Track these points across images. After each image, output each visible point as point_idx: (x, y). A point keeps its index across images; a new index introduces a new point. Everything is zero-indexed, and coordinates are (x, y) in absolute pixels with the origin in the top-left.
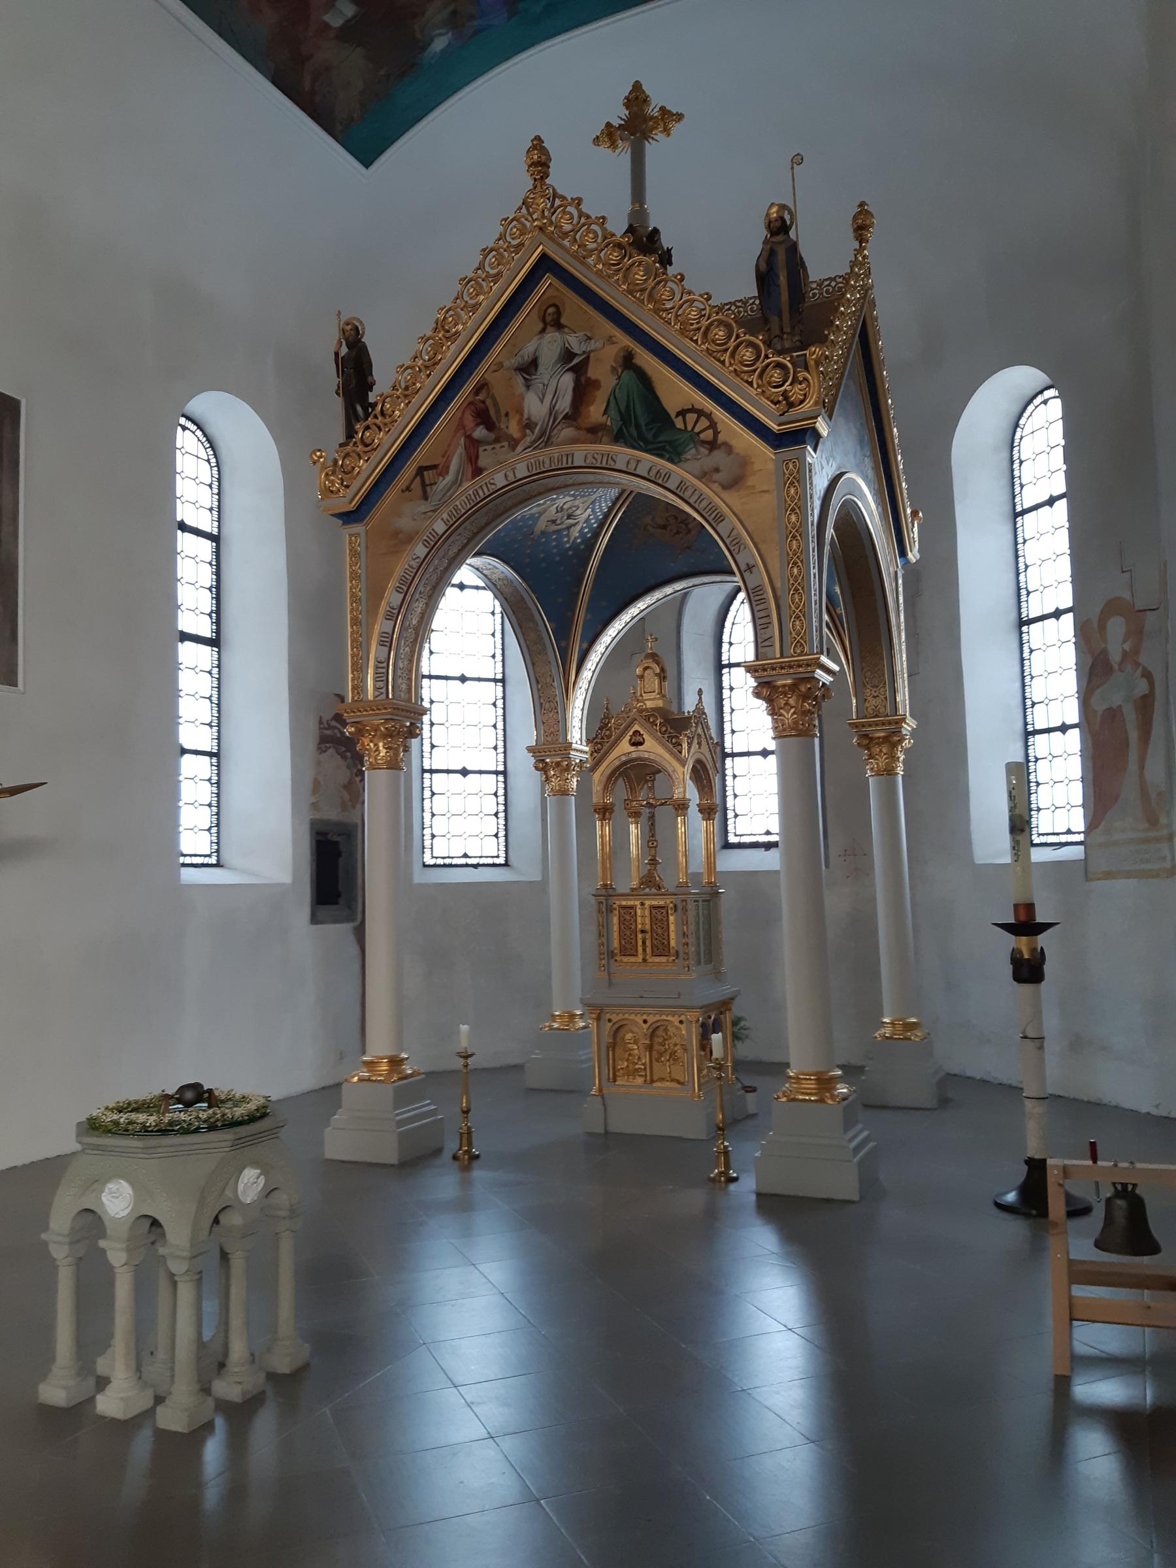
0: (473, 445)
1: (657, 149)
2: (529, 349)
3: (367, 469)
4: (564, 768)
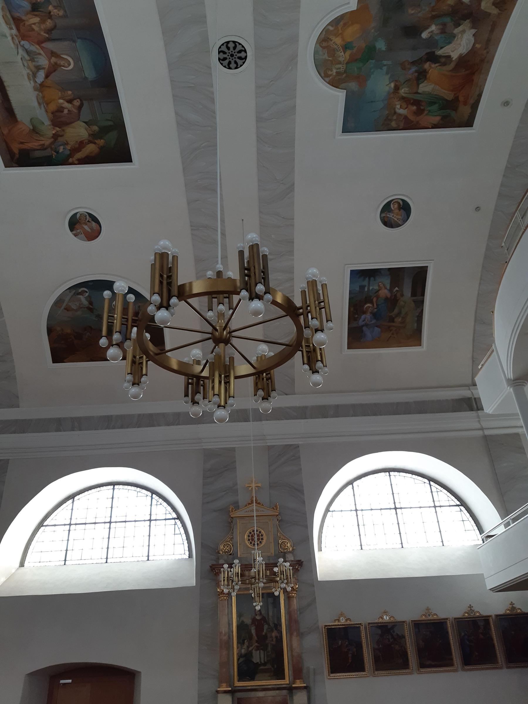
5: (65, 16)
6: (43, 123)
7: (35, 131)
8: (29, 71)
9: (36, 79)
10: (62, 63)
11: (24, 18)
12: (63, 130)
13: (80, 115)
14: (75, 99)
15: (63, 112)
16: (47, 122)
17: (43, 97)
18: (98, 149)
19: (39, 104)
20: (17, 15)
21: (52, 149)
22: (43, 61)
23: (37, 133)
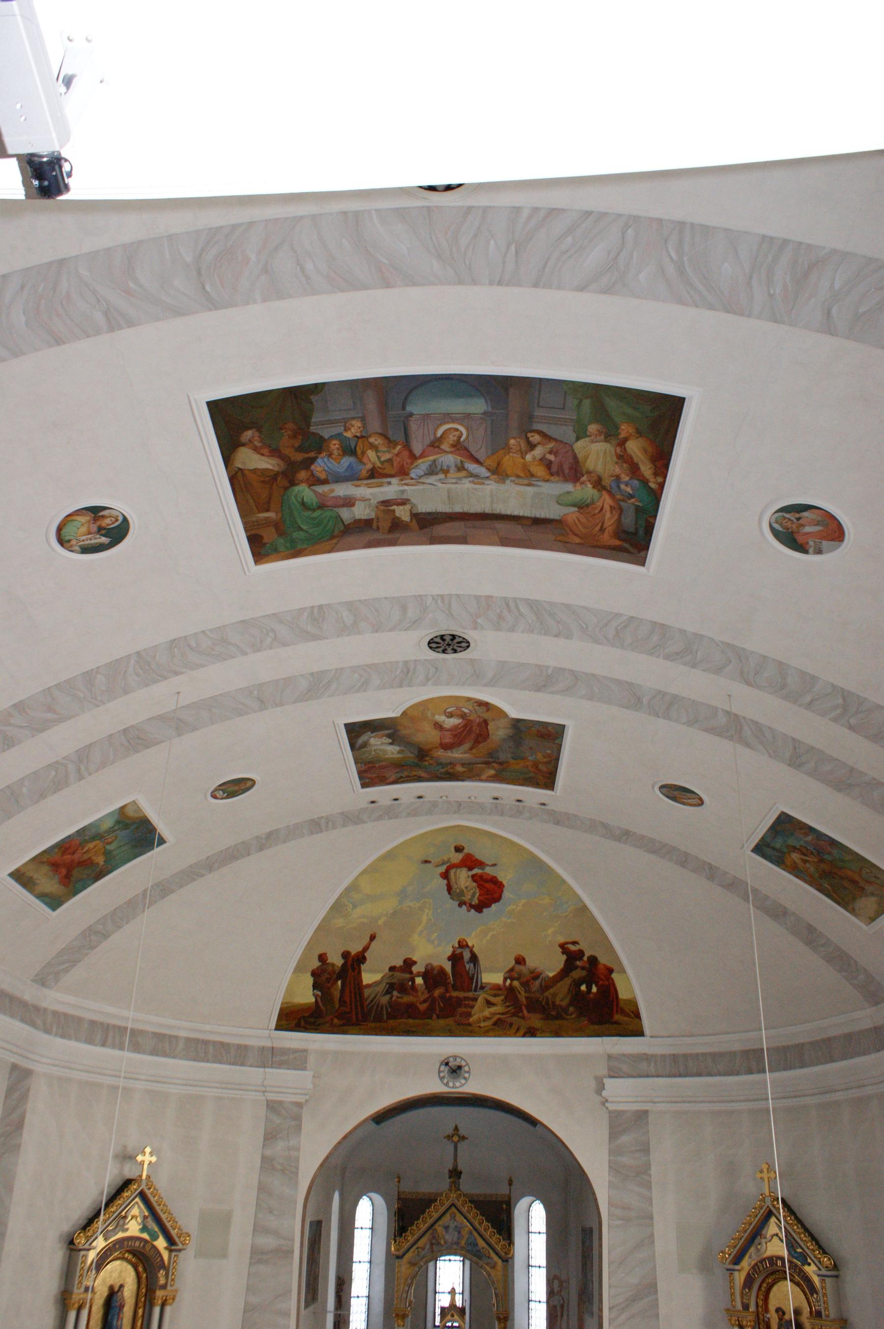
0: (432, 1244)
1: (462, 1146)
2: (447, 1224)
5: (363, 419)
6: (568, 493)
7: (582, 506)
8: (464, 480)
9: (482, 476)
10: (452, 438)
11: (369, 466)
12: (589, 472)
13: (561, 442)
14: (527, 438)
15: (551, 462)
16: (569, 487)
17: (518, 476)
18: (640, 439)
19: (529, 485)
20: (364, 473)
21: (623, 501)
22: (449, 459)
23: (587, 506)
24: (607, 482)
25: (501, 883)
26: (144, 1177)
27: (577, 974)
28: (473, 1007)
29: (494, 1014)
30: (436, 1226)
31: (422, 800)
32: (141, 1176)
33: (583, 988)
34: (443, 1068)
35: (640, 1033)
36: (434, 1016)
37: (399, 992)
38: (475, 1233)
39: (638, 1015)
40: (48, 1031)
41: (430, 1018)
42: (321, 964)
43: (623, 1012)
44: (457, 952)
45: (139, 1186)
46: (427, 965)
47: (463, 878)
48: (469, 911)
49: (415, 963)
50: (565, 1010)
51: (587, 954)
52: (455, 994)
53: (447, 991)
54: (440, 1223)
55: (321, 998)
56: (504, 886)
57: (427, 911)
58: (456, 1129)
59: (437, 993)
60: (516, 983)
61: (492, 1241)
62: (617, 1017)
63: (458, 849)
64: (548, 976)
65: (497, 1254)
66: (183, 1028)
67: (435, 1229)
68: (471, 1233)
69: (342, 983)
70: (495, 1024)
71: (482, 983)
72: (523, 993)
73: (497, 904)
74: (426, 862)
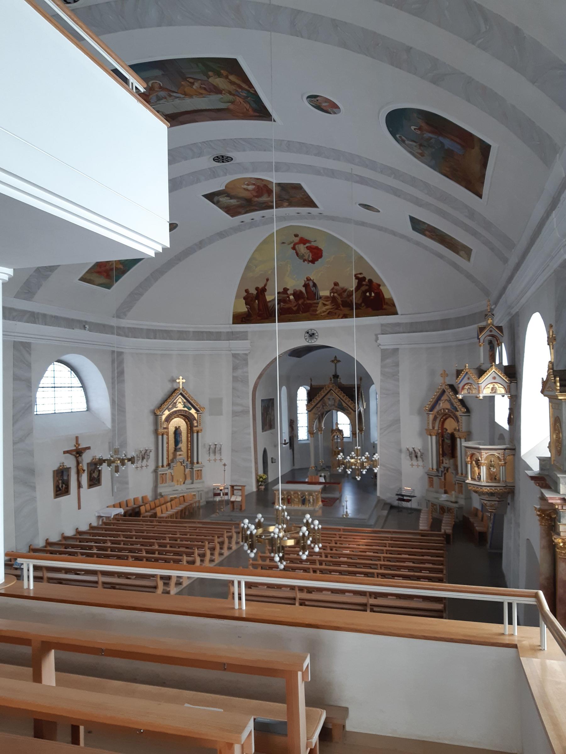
0: (323, 406)
1: (338, 364)
3: (312, 407)
4: (321, 430)
24: (233, 92)
25: (321, 249)
26: (181, 387)
27: (364, 288)
28: (317, 307)
29: (328, 309)
30: (325, 399)
31: (264, 218)
32: (179, 388)
33: (368, 294)
34: (306, 335)
35: (396, 313)
36: (301, 312)
37: (284, 303)
38: (341, 401)
39: (394, 305)
40: (127, 336)
41: (299, 313)
42: (246, 294)
43: (387, 304)
44: (306, 283)
45: (179, 391)
46: (294, 290)
47: (302, 248)
48: (308, 264)
49: (288, 289)
50: (361, 304)
51: (367, 279)
52: (309, 302)
53: (305, 301)
54: (326, 397)
55: (250, 308)
56: (322, 250)
57: (289, 265)
58: (336, 357)
59: (300, 302)
60: (336, 294)
61: (349, 404)
62: (385, 307)
63: (296, 236)
64: (350, 290)
65: (351, 409)
66: (191, 328)
67: (324, 400)
68: (339, 401)
69: (258, 302)
70: (328, 313)
71: (320, 296)
72: (340, 299)
73: (321, 259)
74: (283, 243)
